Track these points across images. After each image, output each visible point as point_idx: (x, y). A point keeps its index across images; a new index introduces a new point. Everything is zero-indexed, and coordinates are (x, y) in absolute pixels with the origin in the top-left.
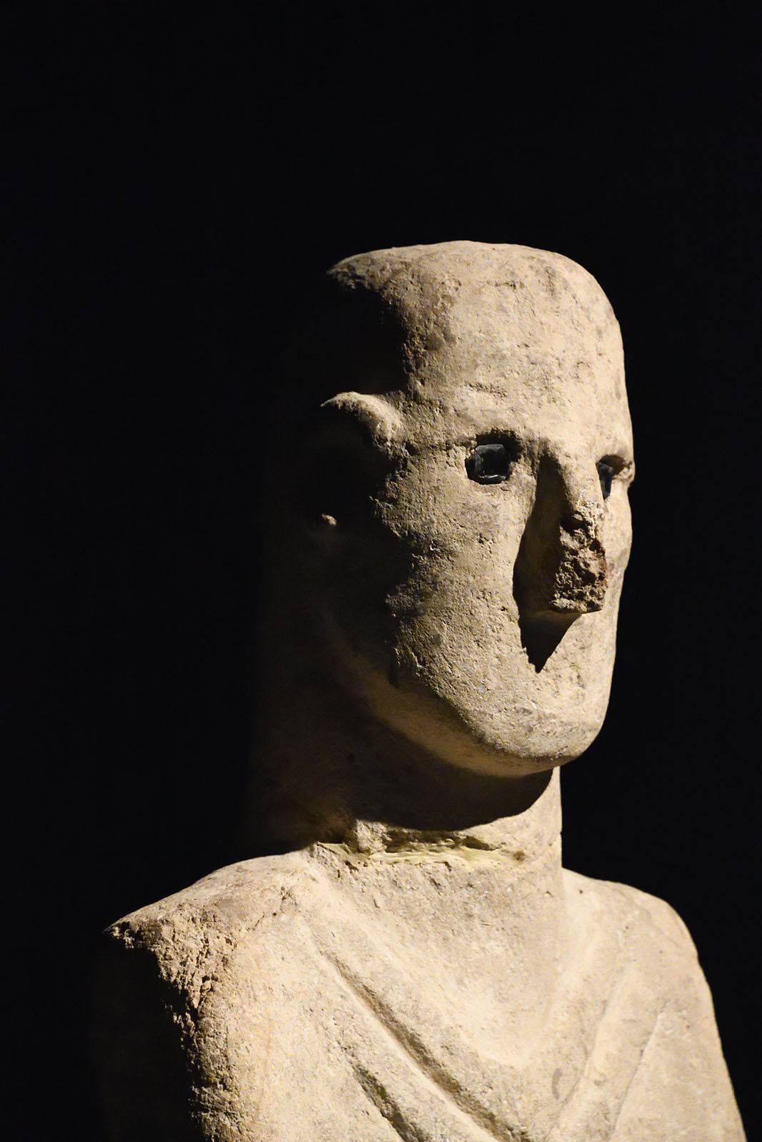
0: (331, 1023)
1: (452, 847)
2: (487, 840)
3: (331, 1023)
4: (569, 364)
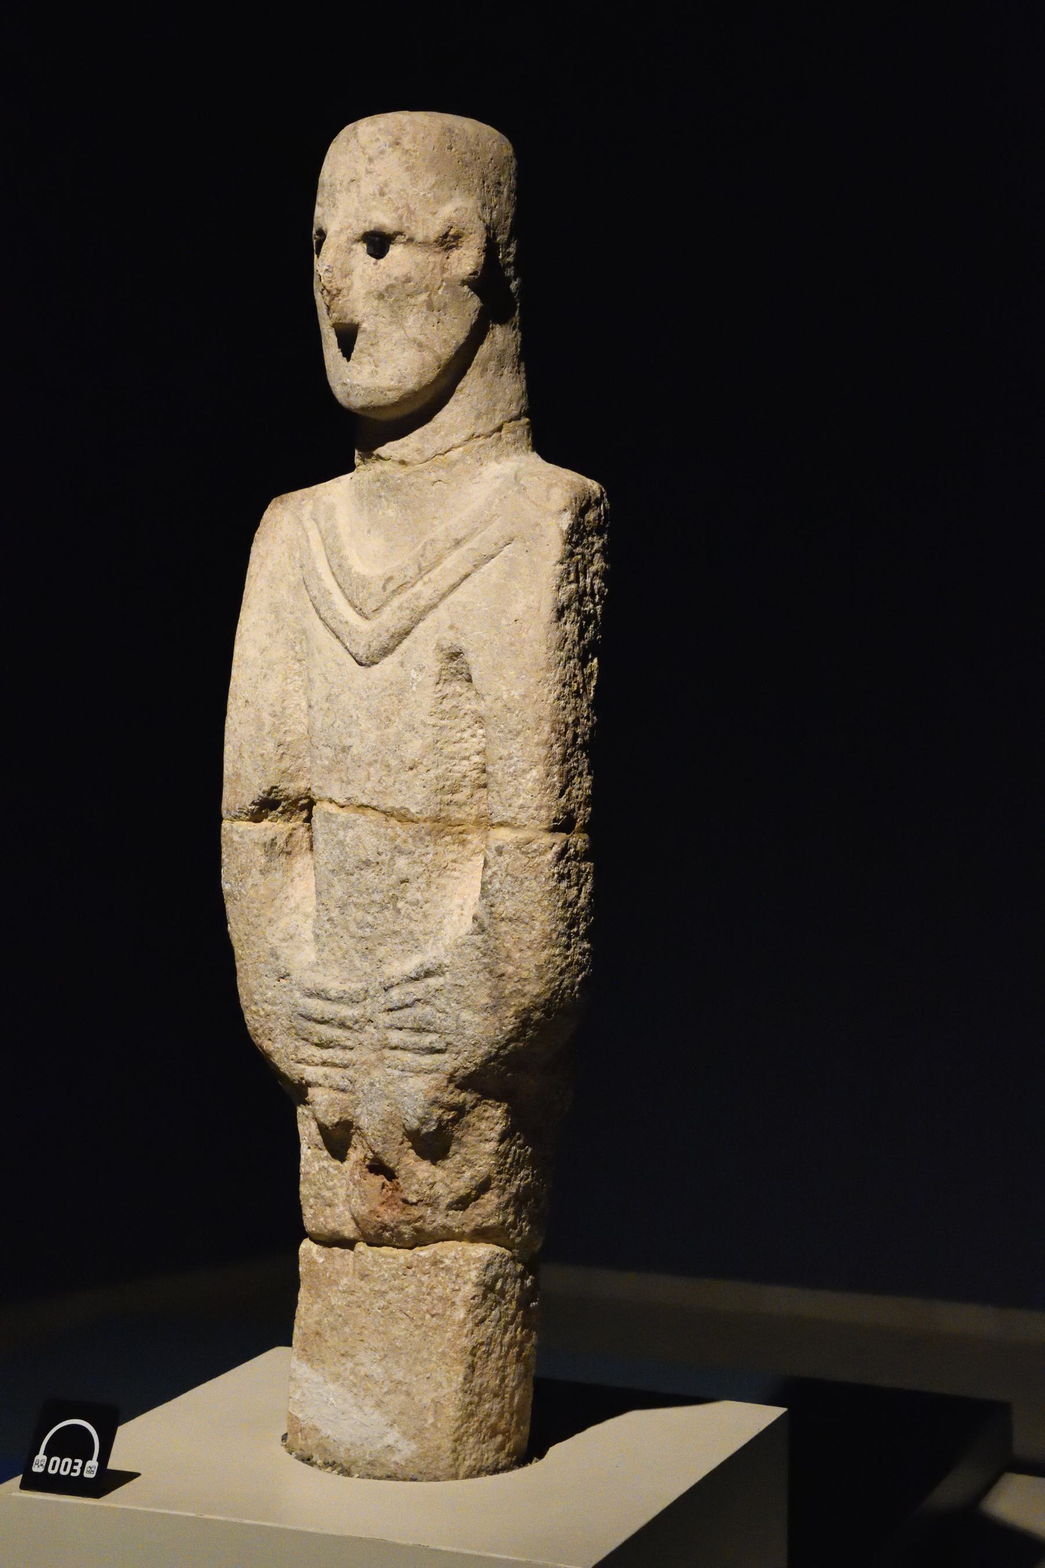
0: (297, 555)
1: (377, 460)
2: (383, 456)
3: (297, 555)
4: (345, 184)
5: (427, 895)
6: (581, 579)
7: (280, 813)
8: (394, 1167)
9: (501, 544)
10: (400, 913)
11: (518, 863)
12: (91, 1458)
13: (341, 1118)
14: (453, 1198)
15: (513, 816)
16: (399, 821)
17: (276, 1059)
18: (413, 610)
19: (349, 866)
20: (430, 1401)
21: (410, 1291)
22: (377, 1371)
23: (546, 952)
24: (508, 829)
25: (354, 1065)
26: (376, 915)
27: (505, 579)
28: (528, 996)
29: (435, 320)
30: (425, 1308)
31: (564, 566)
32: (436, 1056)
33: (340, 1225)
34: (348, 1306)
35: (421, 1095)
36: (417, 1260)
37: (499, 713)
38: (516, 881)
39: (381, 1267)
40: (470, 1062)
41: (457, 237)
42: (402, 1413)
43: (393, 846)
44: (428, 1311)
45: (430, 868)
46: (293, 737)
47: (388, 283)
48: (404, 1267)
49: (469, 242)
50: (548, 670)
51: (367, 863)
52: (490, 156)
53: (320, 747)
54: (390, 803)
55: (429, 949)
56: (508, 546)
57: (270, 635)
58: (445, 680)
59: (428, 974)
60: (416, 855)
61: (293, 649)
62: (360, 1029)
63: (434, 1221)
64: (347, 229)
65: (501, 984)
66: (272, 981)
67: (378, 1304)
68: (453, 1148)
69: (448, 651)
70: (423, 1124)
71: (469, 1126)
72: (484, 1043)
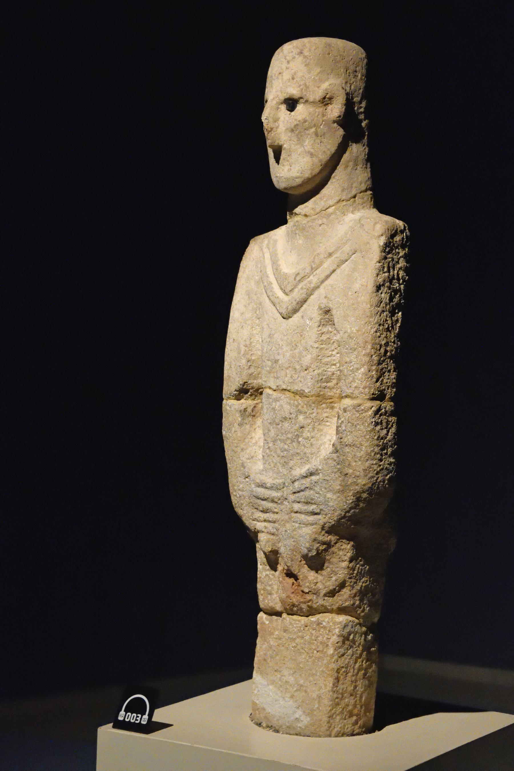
0: (259, 266)
1: (295, 215)
3: (259, 266)
4: (276, 75)
5: (312, 434)
6: (391, 271)
7: (249, 395)
8: (297, 574)
9: (350, 254)
10: (300, 443)
11: (354, 416)
12: (145, 714)
13: (272, 548)
14: (326, 591)
15: (351, 392)
16: (300, 397)
17: (244, 519)
18: (307, 289)
19: (277, 421)
20: (316, 695)
21: (307, 639)
22: (291, 679)
23: (368, 462)
24: (350, 399)
25: (278, 521)
26: (289, 445)
27: (352, 272)
28: (360, 485)
29: (319, 141)
30: (314, 647)
31: (381, 264)
32: (316, 516)
33: (274, 605)
34: (278, 645)
35: (308, 537)
36: (310, 622)
37: (346, 340)
38: (353, 425)
39: (293, 626)
40: (332, 519)
41: (330, 99)
42: (303, 701)
43: (297, 409)
44: (315, 649)
45: (314, 421)
46: (255, 357)
47: (295, 123)
48: (304, 626)
49: (337, 100)
50: (371, 317)
51: (285, 419)
52: (351, 58)
53: (266, 361)
54: (296, 387)
55: (313, 462)
56: (354, 255)
57: (245, 306)
58: (323, 325)
59: (312, 474)
60: (308, 414)
61: (256, 313)
62: (281, 503)
63: (317, 602)
64: (277, 98)
65: (346, 478)
66: (241, 479)
67: (292, 645)
68: (326, 565)
69: (324, 310)
70: (309, 551)
71: (334, 553)
72: (338, 509)
